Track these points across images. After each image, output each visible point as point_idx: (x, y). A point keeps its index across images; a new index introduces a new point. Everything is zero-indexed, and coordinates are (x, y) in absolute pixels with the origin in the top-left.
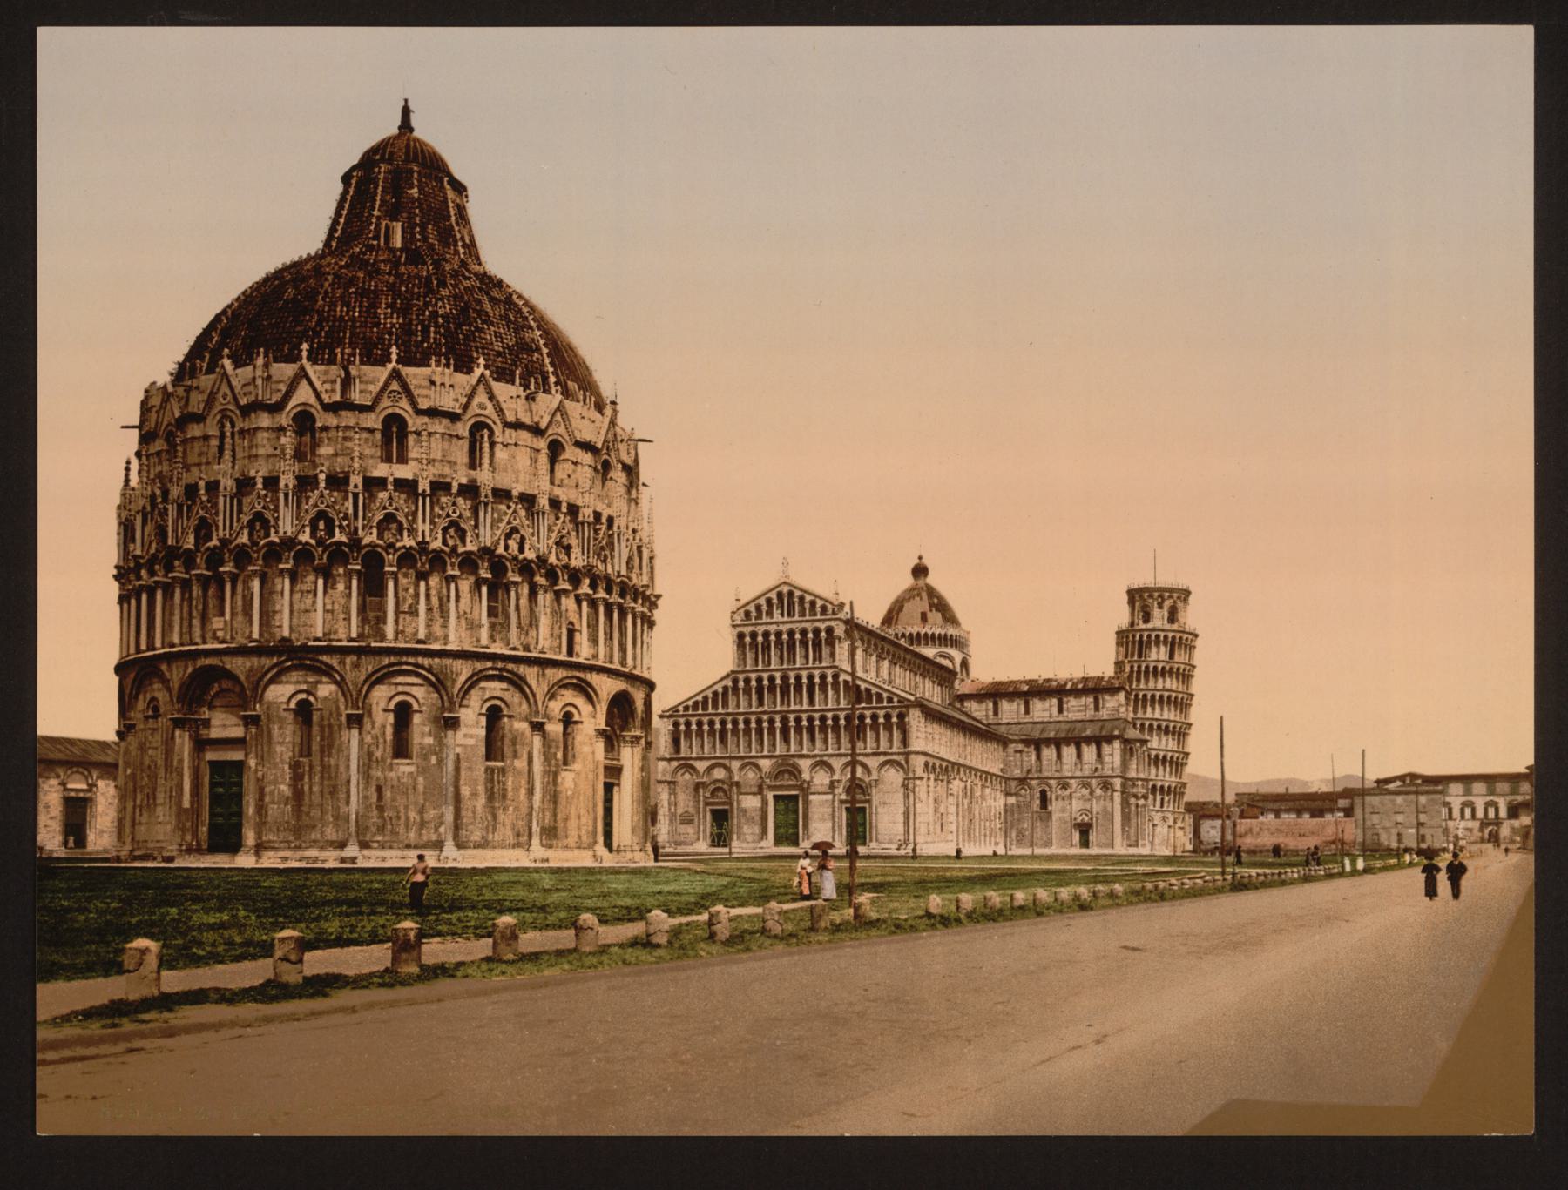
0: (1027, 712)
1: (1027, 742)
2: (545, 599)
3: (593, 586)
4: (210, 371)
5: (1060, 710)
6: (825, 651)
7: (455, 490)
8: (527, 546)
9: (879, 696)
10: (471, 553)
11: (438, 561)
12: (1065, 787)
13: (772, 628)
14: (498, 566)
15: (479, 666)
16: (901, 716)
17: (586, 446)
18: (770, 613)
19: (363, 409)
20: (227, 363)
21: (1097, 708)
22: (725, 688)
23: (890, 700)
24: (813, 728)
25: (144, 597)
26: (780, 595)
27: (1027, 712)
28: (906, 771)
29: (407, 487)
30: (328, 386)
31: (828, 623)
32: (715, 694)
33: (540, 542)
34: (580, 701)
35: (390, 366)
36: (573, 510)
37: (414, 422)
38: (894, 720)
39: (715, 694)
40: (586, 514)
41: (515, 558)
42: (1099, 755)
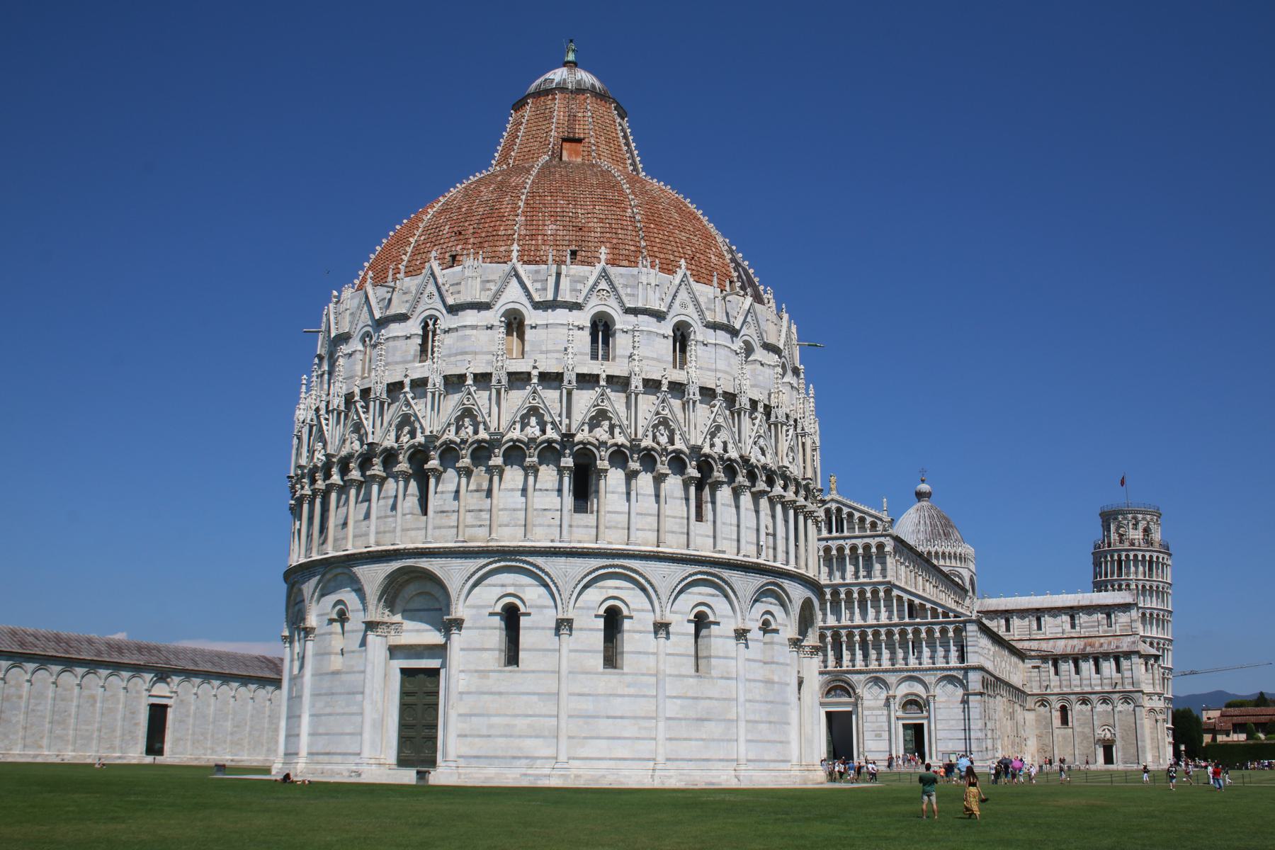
0: (1039, 628)
1: (1044, 659)
2: (746, 499)
3: (785, 488)
4: (407, 274)
5: (1073, 626)
6: (877, 567)
7: (664, 388)
8: (730, 446)
9: (934, 611)
10: (681, 452)
11: (648, 459)
12: (1084, 702)
14: (705, 465)
15: (691, 569)
16: (958, 631)
17: (769, 347)
19: (576, 306)
20: (435, 265)
23: (945, 615)
24: (868, 641)
25: (318, 501)
26: (828, 511)
27: (1039, 628)
28: (965, 687)
29: (618, 383)
30: (539, 285)
31: (878, 540)
33: (746, 440)
34: (777, 610)
35: (599, 267)
36: (768, 410)
37: (622, 322)
38: (951, 634)
40: (781, 413)
41: (721, 458)
42: (1118, 670)
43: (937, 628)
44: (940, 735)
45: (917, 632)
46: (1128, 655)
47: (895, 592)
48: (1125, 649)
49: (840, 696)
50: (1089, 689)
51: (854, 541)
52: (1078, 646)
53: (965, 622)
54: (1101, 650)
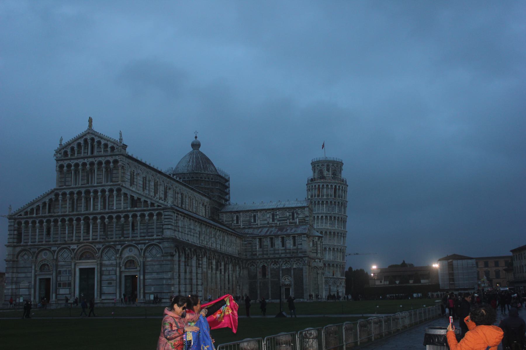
5: (273, 220)
9: (146, 202)
12: (276, 263)
13: (80, 162)
18: (79, 152)
21: (293, 219)
22: (51, 200)
26: (86, 141)
31: (114, 158)
32: (45, 203)
39: (45, 203)
42: (294, 244)
43: (147, 213)
44: (148, 282)
45: (134, 216)
46: (300, 235)
47: (123, 191)
48: (299, 232)
49: (89, 259)
50: (277, 256)
51: (100, 159)
52: (274, 230)
53: (163, 209)
54: (285, 233)
